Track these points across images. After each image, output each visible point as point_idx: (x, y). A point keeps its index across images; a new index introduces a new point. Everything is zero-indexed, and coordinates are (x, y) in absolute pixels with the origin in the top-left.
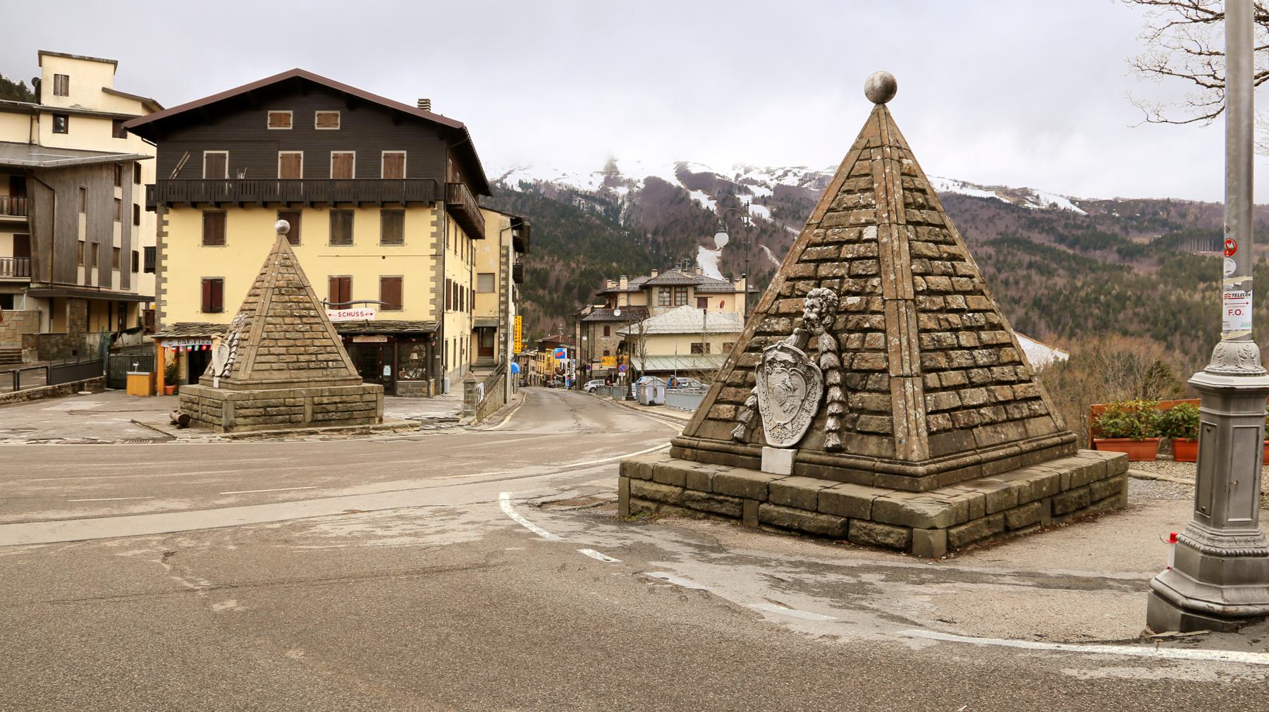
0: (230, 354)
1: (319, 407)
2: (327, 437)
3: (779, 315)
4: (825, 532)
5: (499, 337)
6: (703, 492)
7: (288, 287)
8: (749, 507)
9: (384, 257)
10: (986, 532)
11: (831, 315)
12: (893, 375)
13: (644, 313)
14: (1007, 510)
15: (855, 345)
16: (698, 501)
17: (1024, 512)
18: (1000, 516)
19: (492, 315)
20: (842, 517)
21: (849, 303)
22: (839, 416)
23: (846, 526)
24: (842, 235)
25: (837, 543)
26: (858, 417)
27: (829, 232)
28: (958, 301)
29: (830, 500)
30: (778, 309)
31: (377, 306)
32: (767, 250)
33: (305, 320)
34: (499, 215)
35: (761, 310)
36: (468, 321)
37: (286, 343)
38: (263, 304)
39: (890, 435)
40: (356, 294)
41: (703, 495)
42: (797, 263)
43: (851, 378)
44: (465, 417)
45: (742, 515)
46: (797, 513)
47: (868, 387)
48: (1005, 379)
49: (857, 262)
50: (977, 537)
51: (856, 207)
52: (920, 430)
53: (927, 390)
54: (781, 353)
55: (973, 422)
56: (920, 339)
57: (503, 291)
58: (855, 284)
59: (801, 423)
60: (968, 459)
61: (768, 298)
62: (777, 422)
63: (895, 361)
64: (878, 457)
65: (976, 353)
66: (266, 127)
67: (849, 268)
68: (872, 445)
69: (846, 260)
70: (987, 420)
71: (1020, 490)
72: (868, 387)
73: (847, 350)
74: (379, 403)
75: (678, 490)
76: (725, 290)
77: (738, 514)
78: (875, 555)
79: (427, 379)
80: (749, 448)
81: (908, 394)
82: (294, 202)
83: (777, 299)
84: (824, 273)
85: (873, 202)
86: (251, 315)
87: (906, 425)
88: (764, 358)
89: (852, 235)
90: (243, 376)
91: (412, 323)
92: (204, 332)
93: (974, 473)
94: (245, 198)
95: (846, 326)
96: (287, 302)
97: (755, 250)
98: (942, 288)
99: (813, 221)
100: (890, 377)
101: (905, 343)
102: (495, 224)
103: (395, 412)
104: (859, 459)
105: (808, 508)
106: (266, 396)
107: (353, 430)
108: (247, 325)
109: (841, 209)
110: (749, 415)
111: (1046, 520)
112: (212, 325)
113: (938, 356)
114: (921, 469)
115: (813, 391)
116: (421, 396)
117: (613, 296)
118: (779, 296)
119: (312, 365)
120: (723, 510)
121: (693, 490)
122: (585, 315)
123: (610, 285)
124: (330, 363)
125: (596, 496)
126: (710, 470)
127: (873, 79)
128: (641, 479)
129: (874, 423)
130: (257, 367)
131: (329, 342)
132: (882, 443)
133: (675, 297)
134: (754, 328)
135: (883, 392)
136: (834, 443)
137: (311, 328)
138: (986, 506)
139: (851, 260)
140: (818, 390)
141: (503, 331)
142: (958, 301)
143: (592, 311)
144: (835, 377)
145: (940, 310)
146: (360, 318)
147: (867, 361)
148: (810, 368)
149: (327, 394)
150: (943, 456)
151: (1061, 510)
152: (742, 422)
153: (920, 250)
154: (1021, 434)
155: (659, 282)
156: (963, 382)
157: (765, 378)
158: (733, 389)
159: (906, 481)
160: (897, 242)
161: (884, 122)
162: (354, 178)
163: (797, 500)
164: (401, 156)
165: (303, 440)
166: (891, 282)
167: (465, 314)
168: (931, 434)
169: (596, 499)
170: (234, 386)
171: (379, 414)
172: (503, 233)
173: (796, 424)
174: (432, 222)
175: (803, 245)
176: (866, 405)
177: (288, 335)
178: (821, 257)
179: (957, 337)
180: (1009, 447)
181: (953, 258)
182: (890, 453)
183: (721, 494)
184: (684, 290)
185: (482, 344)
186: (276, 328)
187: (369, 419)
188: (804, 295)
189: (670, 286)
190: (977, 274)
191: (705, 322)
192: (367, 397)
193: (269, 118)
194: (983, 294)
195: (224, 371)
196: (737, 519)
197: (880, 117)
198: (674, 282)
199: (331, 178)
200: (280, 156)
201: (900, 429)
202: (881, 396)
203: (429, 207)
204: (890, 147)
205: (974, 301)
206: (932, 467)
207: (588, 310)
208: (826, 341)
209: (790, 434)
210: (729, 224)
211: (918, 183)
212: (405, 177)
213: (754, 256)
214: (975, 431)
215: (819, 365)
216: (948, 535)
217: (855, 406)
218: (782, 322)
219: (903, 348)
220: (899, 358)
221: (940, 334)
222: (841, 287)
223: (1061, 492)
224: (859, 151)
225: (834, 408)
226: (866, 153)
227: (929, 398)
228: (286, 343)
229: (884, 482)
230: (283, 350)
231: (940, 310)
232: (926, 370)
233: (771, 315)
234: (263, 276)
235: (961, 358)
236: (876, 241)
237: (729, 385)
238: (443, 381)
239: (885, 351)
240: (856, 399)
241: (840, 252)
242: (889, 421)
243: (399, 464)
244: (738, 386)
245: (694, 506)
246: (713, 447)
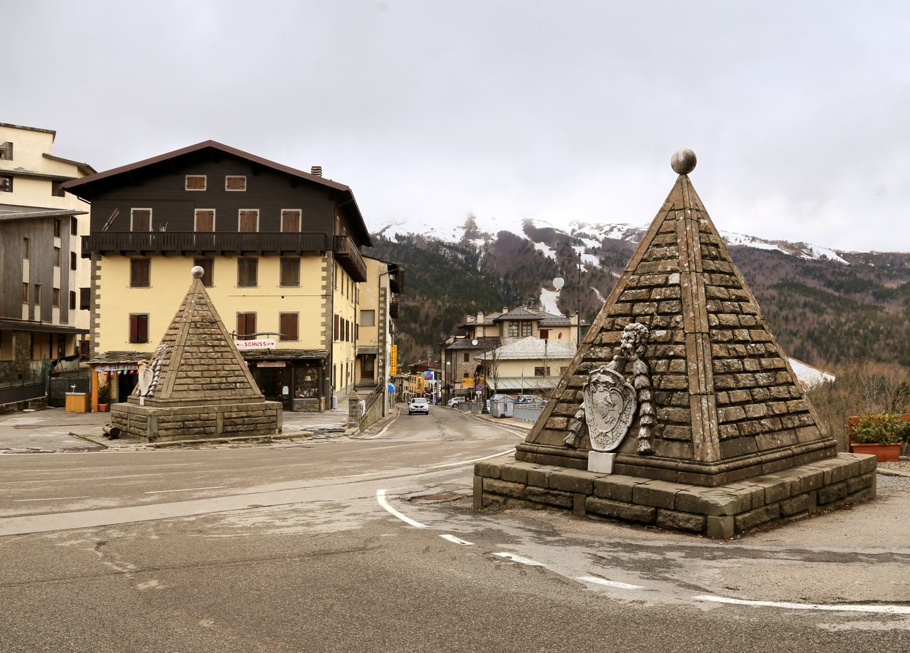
0: (154, 377)
1: (228, 421)
2: (235, 445)
3: (602, 345)
4: (638, 519)
5: (378, 362)
6: (541, 487)
7: (202, 321)
8: (578, 500)
9: (283, 297)
10: (766, 518)
11: (643, 345)
12: (692, 393)
13: (496, 342)
14: (782, 500)
15: (662, 369)
16: (537, 495)
17: (795, 502)
18: (777, 506)
19: (372, 344)
20: (652, 507)
21: (658, 335)
22: (649, 426)
23: (655, 514)
24: (653, 280)
25: (648, 528)
26: (665, 427)
27: (642, 278)
28: (743, 334)
29: (642, 493)
30: (601, 340)
31: (277, 337)
32: (597, 292)
33: (217, 349)
34: (378, 262)
35: (588, 340)
36: (352, 350)
37: (200, 368)
38: (181, 335)
39: (689, 441)
40: (259, 328)
41: (542, 490)
42: (617, 303)
43: (659, 395)
44: (349, 428)
46: (616, 504)
47: (673, 403)
48: (781, 396)
49: (664, 302)
50: (758, 522)
51: (663, 258)
52: (713, 437)
53: (719, 405)
55: (755, 430)
56: (713, 365)
57: (381, 325)
58: (662, 320)
59: (620, 432)
60: (751, 460)
61: (594, 331)
62: (600, 431)
63: (693, 382)
64: (681, 459)
65: (757, 375)
66: (184, 189)
67: (658, 307)
68: (676, 450)
69: (655, 300)
70: (766, 429)
71: (792, 484)
72: (673, 403)
73: (656, 373)
74: (279, 417)
75: (521, 486)
76: (562, 324)
77: (569, 505)
78: (677, 537)
79: (318, 397)
80: (578, 452)
81: (704, 408)
82: (207, 251)
83: (600, 332)
84: (638, 311)
85: (677, 254)
86: (172, 345)
87: (702, 433)
88: (590, 379)
89: (660, 280)
90: (164, 395)
91: (306, 352)
92: (131, 359)
93: (756, 472)
94: (165, 248)
95: (655, 354)
96: (201, 334)
97: (587, 291)
98: (731, 323)
99: (629, 269)
100: (690, 395)
101: (701, 368)
102: (375, 269)
103: (291, 425)
104: (665, 460)
105: (624, 500)
106: (184, 412)
107: (257, 439)
108: (168, 353)
109: (651, 259)
110: (578, 425)
111: (813, 508)
112: (139, 353)
113: (727, 378)
114: (714, 469)
115: (629, 407)
116: (314, 411)
117: (472, 328)
118: (602, 329)
119: (223, 386)
120: (558, 502)
121: (534, 486)
122: (449, 345)
123: (470, 320)
124: (238, 385)
125: (455, 492)
126: (547, 470)
127: (678, 155)
128: (491, 478)
129: (677, 432)
130: (176, 388)
131: (238, 367)
132: (683, 448)
133: (522, 330)
136: (646, 448)
137: (222, 355)
138: (765, 497)
139: (659, 301)
140: (633, 405)
141: (381, 357)
142: (743, 334)
143: (455, 341)
144: (646, 395)
145: (729, 342)
146: (263, 347)
147: (671, 382)
148: (626, 388)
149: (235, 410)
150: (731, 458)
151: (824, 500)
152: (573, 432)
153: (714, 293)
154: (793, 440)
155: (509, 318)
156: (748, 398)
157: (591, 396)
158: (565, 405)
159: (703, 478)
160: (696, 286)
161: (686, 189)
162: (258, 231)
163: (616, 493)
164: (297, 214)
165: (215, 448)
166: (691, 318)
167: (350, 344)
168: (722, 440)
169: (455, 494)
170: (157, 404)
171: (279, 426)
172: (381, 277)
173: (616, 433)
174: (323, 268)
175: (621, 288)
176: (670, 418)
177: (203, 362)
178: (635, 298)
179: (743, 363)
180: (783, 450)
181: (740, 299)
182: (689, 456)
183: (556, 489)
184: (529, 323)
185: (364, 368)
186: (192, 355)
187: (270, 430)
188: (622, 328)
189: (518, 321)
190: (758, 312)
191: (546, 350)
192: (269, 413)
193: (186, 181)
194: (763, 328)
195: (149, 392)
196: (569, 509)
197: (683, 185)
198: (521, 318)
199: (239, 231)
200: (195, 213)
201: (698, 436)
202: (683, 410)
203: (320, 256)
204: (691, 209)
205: (756, 335)
206: (723, 466)
207: (451, 340)
208: (639, 366)
209: (611, 441)
210: (566, 270)
211: (712, 239)
212: (300, 231)
213: (586, 296)
214: (757, 438)
215: (633, 385)
216: (735, 519)
217: (662, 418)
218: (605, 351)
219: (700, 372)
220: (697, 380)
221: (729, 360)
222: (651, 322)
223: (824, 486)
224: (665, 213)
225: (645, 420)
226: (672, 214)
227: (720, 412)
228: (200, 368)
229: (685, 478)
230: (198, 374)
231: (729, 342)
232: (718, 389)
233: (596, 345)
234: (182, 313)
235: (746, 380)
236: (679, 285)
237: (562, 401)
238: (332, 398)
239: (686, 374)
240: (663, 412)
241: (651, 294)
242: (689, 430)
243: (295, 467)
244: (569, 402)
245: (534, 499)
246: (550, 451)
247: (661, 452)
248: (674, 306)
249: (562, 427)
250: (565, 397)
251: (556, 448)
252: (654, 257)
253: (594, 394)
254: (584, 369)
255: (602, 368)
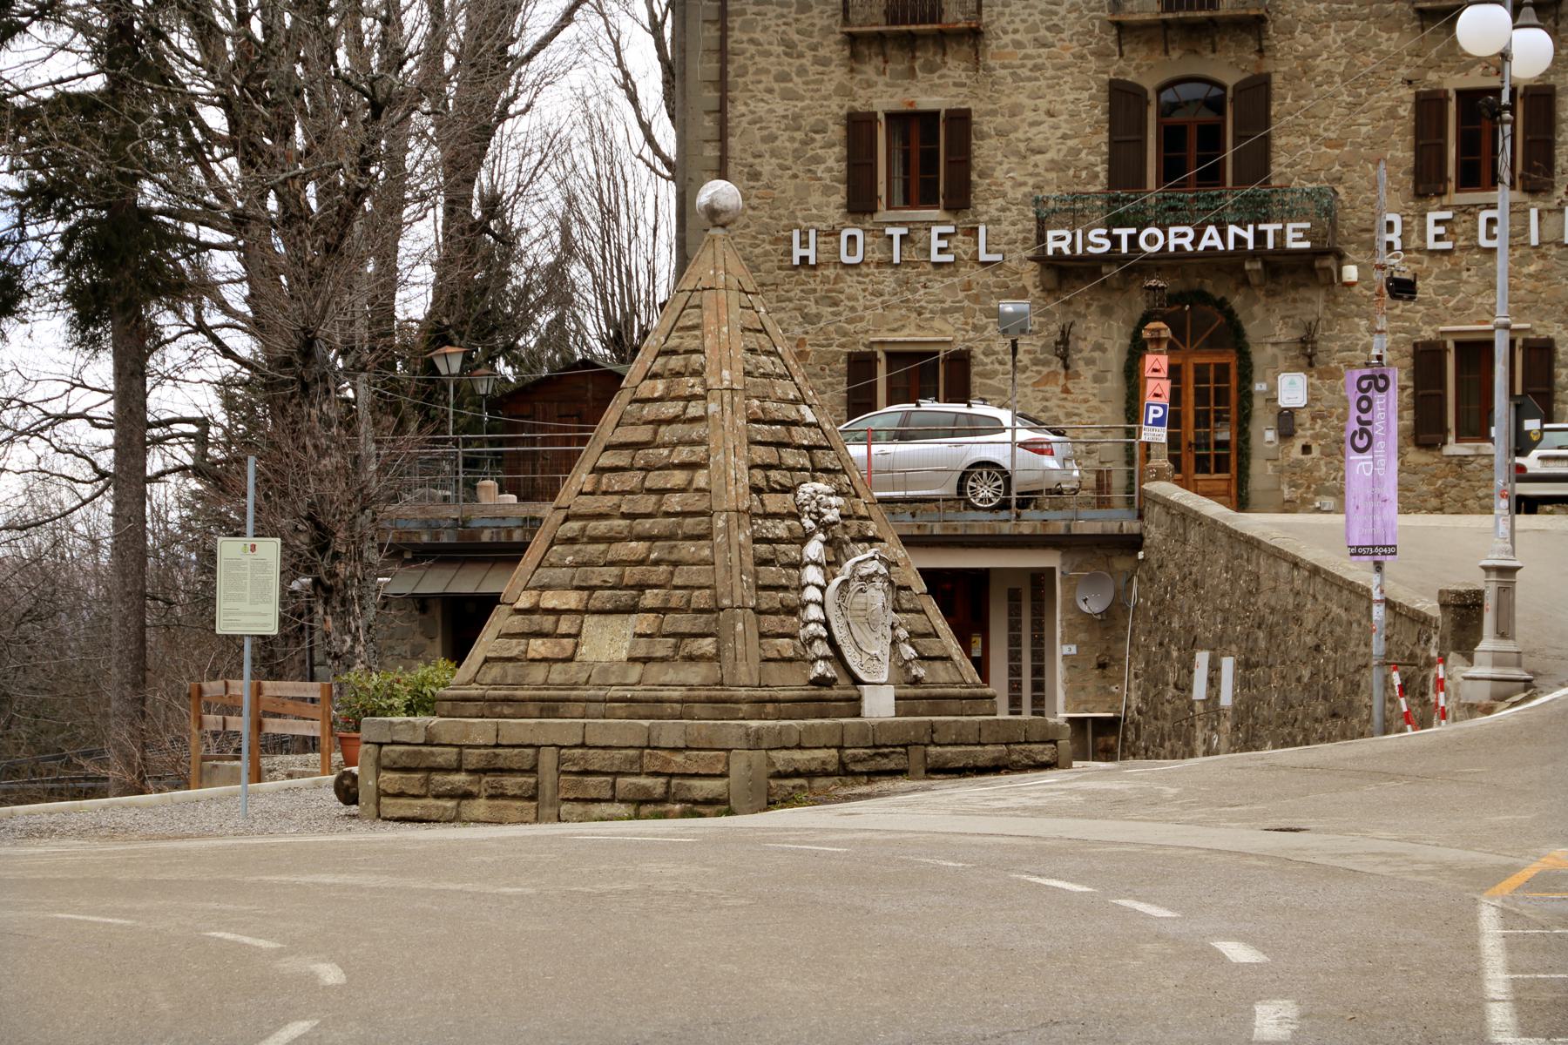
8: (917, 754)
16: (864, 760)
120: (892, 766)
139: (809, 448)
183: (886, 746)
245: (859, 768)
252: (762, 370)
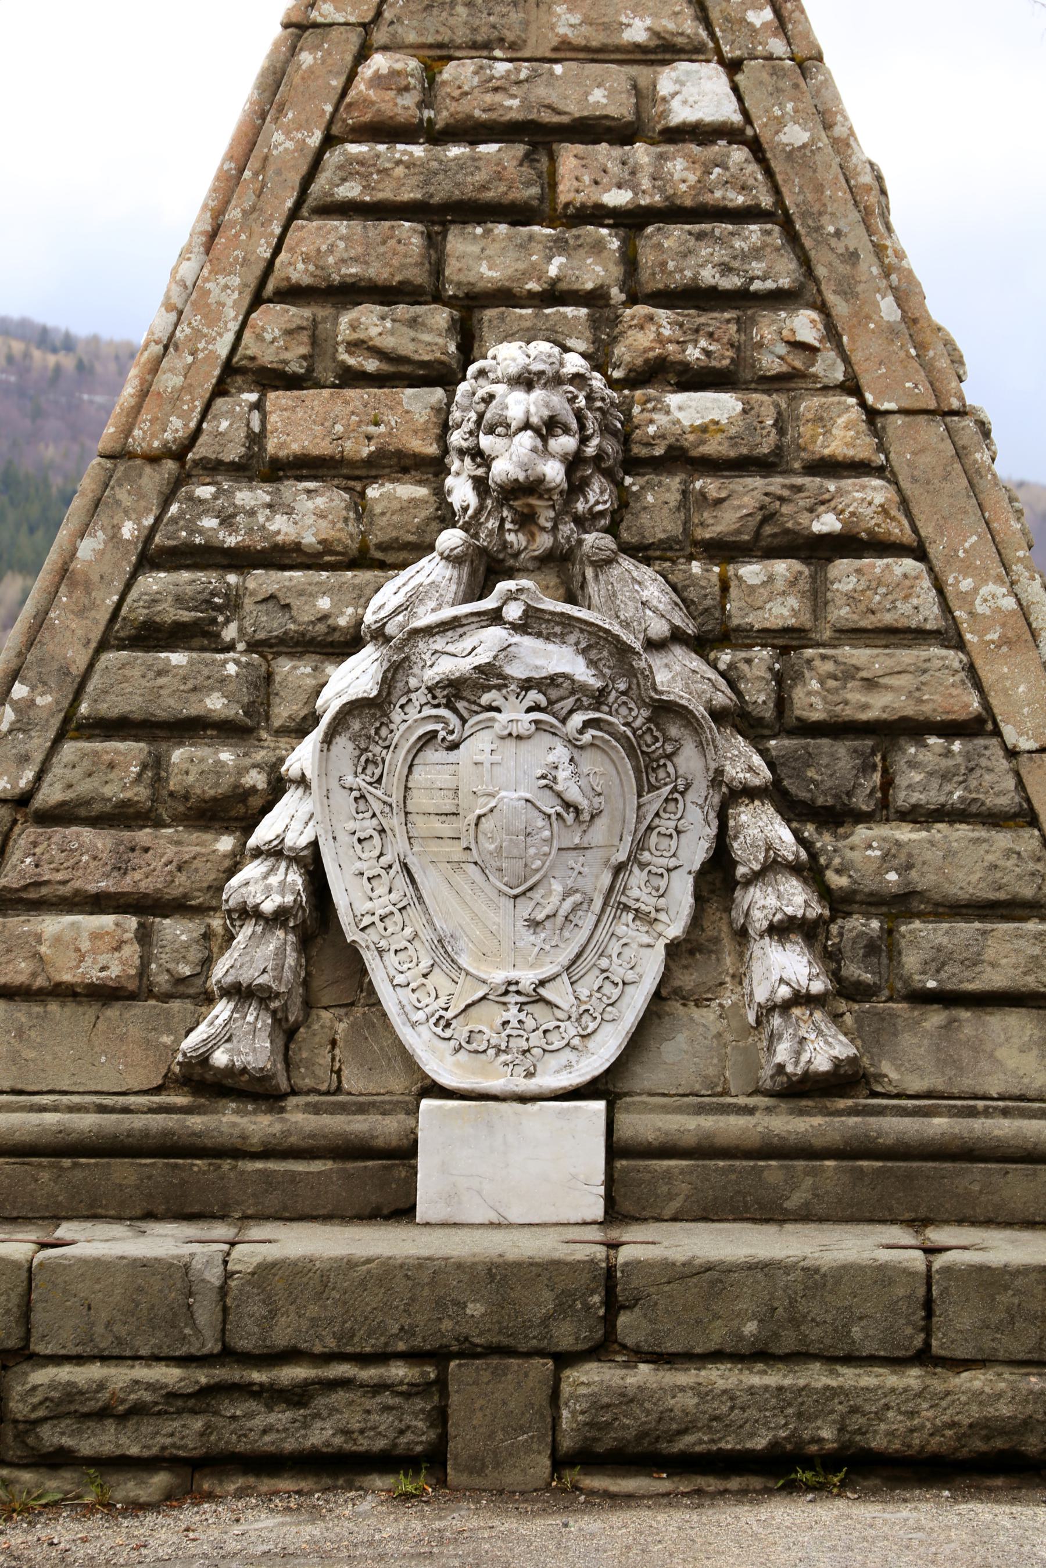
43: (809, 759)
45: (443, 1438)
47: (903, 798)
54: (527, 642)
62: (499, 976)
72: (903, 798)
100: (1012, 754)
104: (972, 1113)
115: (667, 825)
134: (128, 530)
135: (995, 819)
147: (871, 684)
166: (891, 332)
176: (923, 879)
209: (570, 1030)
233: (213, 468)
247: (916, 1069)
248: (756, 253)
249: (115, 971)
250: (85, 788)
251: (102, 1109)
253: (433, 755)
254: (186, 616)
255: (511, 597)
